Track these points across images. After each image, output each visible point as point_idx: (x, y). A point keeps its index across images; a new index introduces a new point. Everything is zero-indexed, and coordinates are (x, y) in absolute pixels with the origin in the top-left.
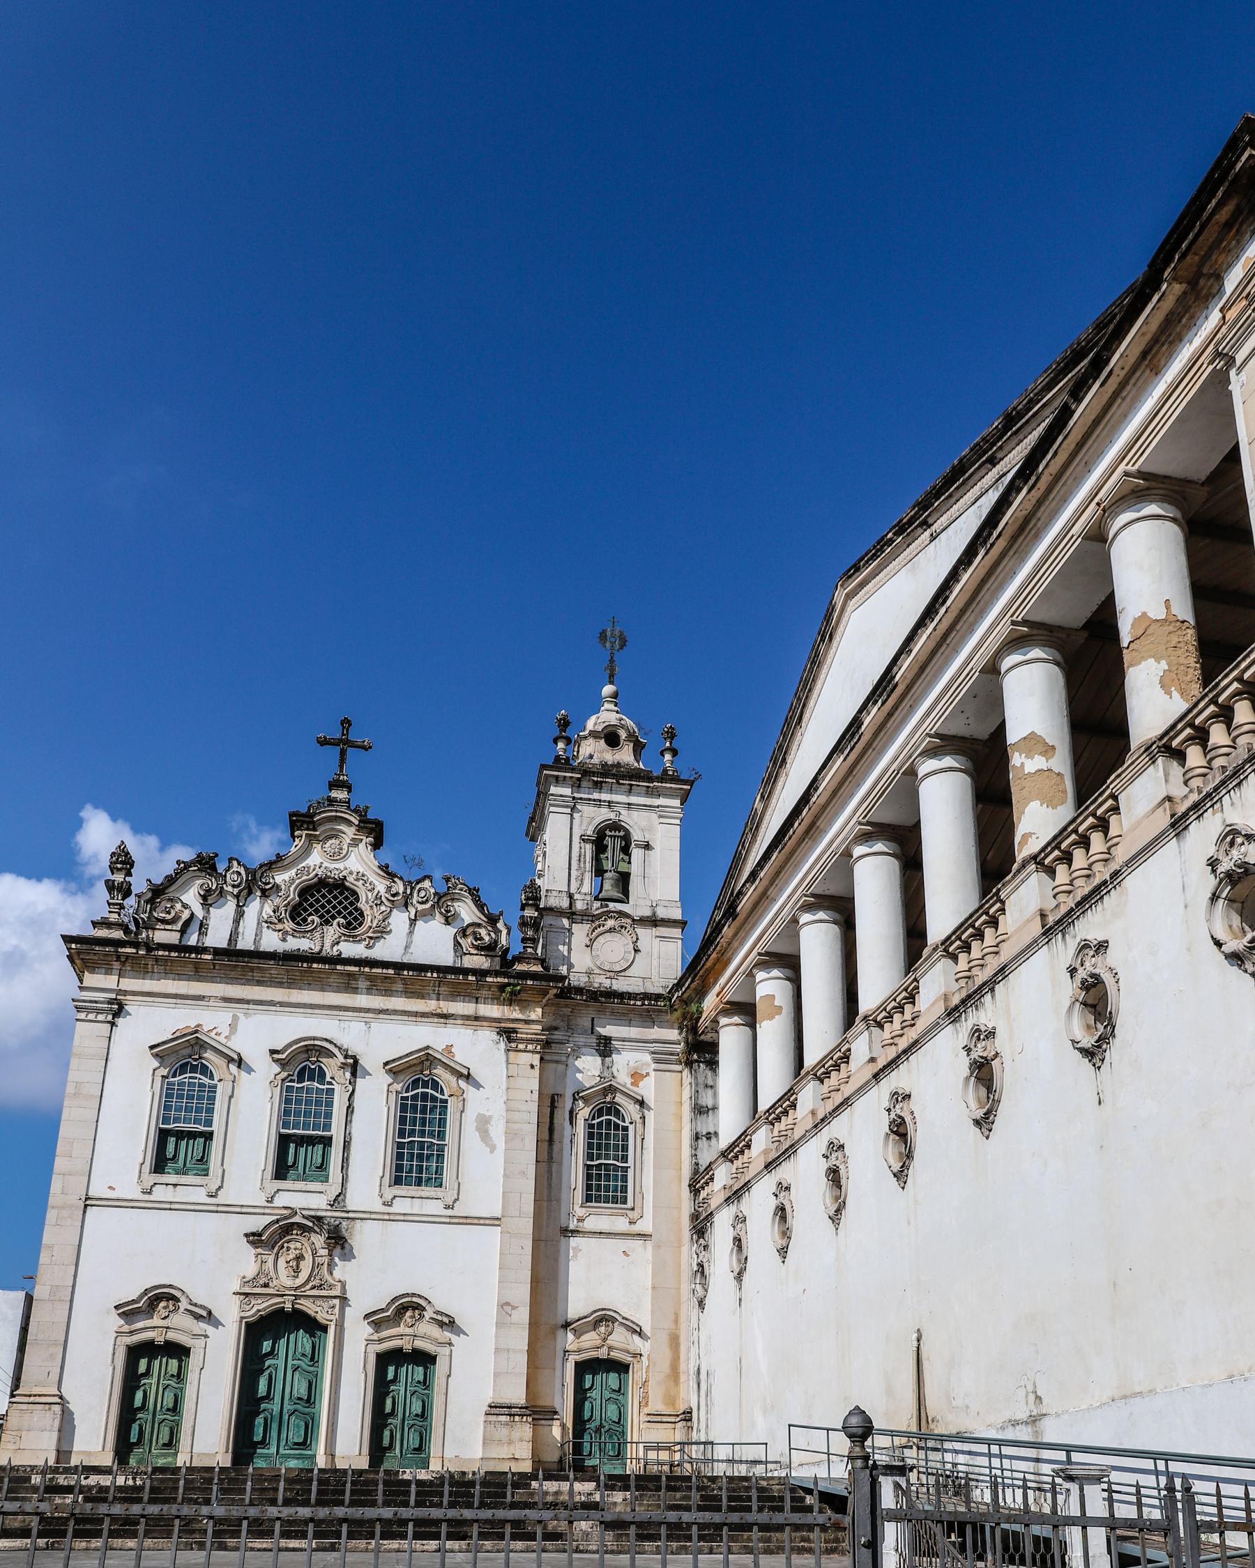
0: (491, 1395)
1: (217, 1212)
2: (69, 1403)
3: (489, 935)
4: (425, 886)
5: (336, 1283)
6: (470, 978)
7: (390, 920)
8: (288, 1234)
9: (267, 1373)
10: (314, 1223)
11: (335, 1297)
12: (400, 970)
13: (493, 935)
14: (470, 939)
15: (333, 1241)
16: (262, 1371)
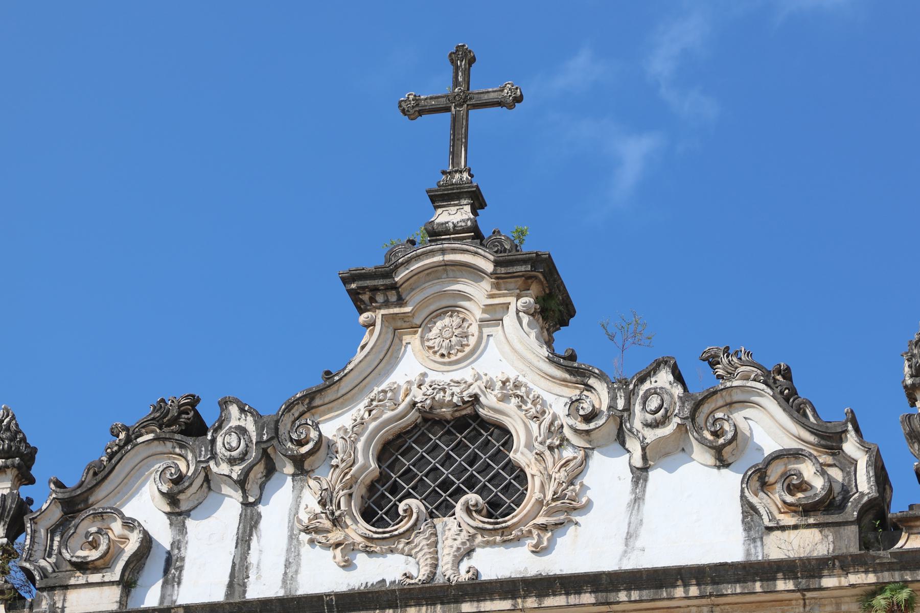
3: (823, 473)
4: (659, 385)
6: (781, 585)
7: (587, 479)
12: (607, 591)
13: (836, 474)
14: (779, 495)
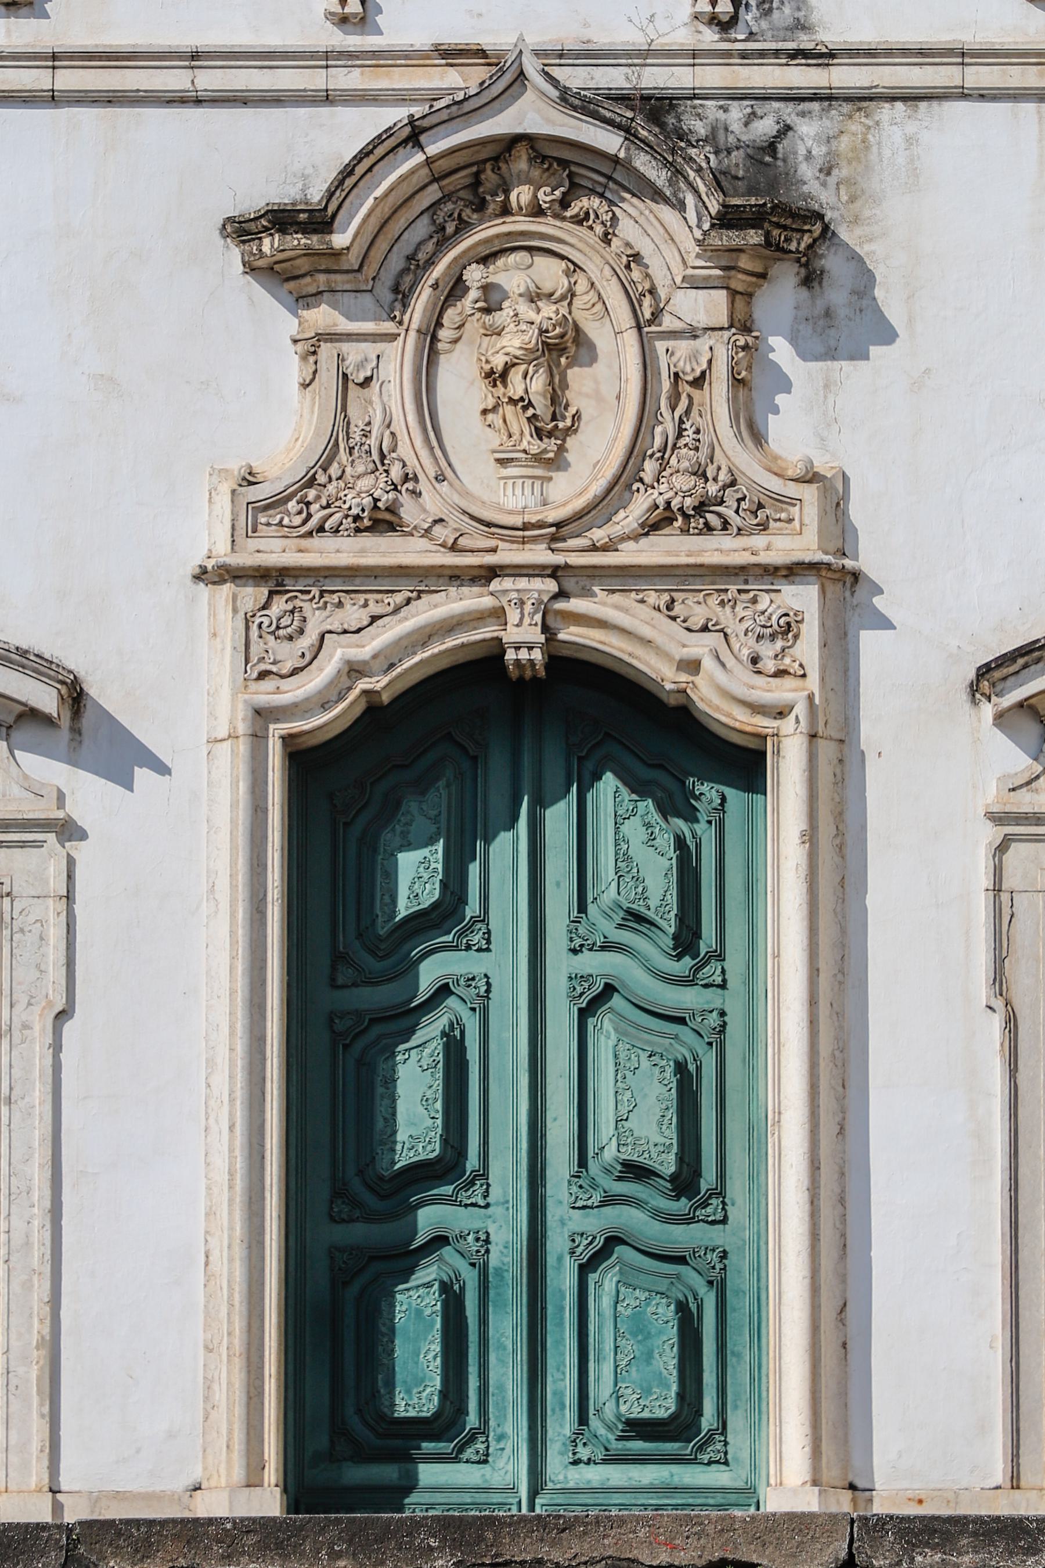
1: (53, 99)
5: (792, 490)
8: (480, 206)
10: (628, 131)
11: (793, 571)
15: (754, 237)
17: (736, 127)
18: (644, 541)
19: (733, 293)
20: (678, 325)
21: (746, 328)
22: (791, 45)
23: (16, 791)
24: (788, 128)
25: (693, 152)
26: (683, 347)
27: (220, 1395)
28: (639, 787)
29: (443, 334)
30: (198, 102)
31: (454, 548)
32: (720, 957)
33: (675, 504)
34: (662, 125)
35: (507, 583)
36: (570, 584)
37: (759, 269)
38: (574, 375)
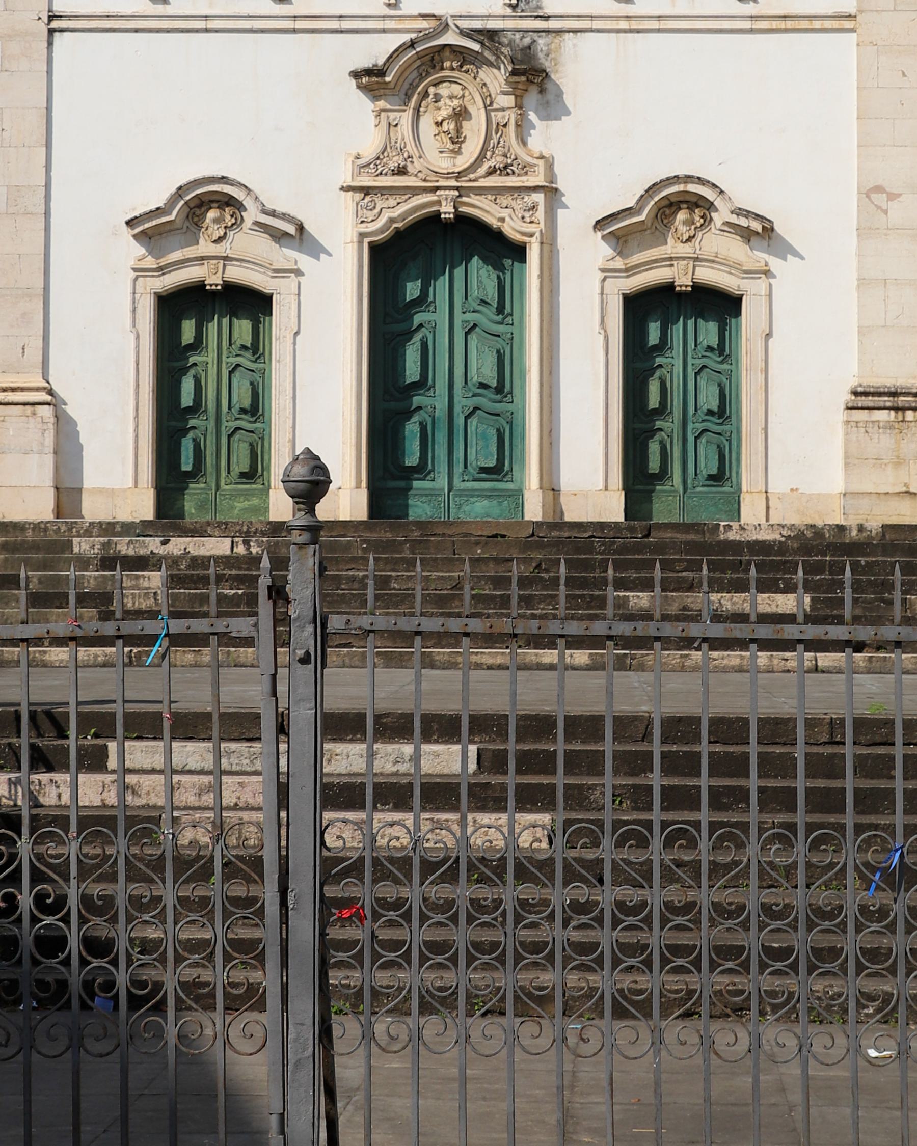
0: (855, 369)
1: (294, 31)
2: (65, 404)
5: (535, 161)
9: (417, 338)
10: (482, 44)
11: (536, 189)
15: (523, 79)
16: (408, 334)
17: (517, 41)
18: (487, 179)
19: (516, 96)
20: (498, 107)
21: (520, 108)
22: (536, 14)
23: (281, 259)
24: (535, 41)
25: (503, 49)
26: (500, 114)
27: (347, 458)
28: (485, 260)
29: (421, 109)
30: (342, 32)
31: (425, 180)
32: (512, 315)
33: (497, 166)
34: (493, 41)
35: (442, 192)
36: (463, 192)
37: (525, 88)
38: (464, 123)
